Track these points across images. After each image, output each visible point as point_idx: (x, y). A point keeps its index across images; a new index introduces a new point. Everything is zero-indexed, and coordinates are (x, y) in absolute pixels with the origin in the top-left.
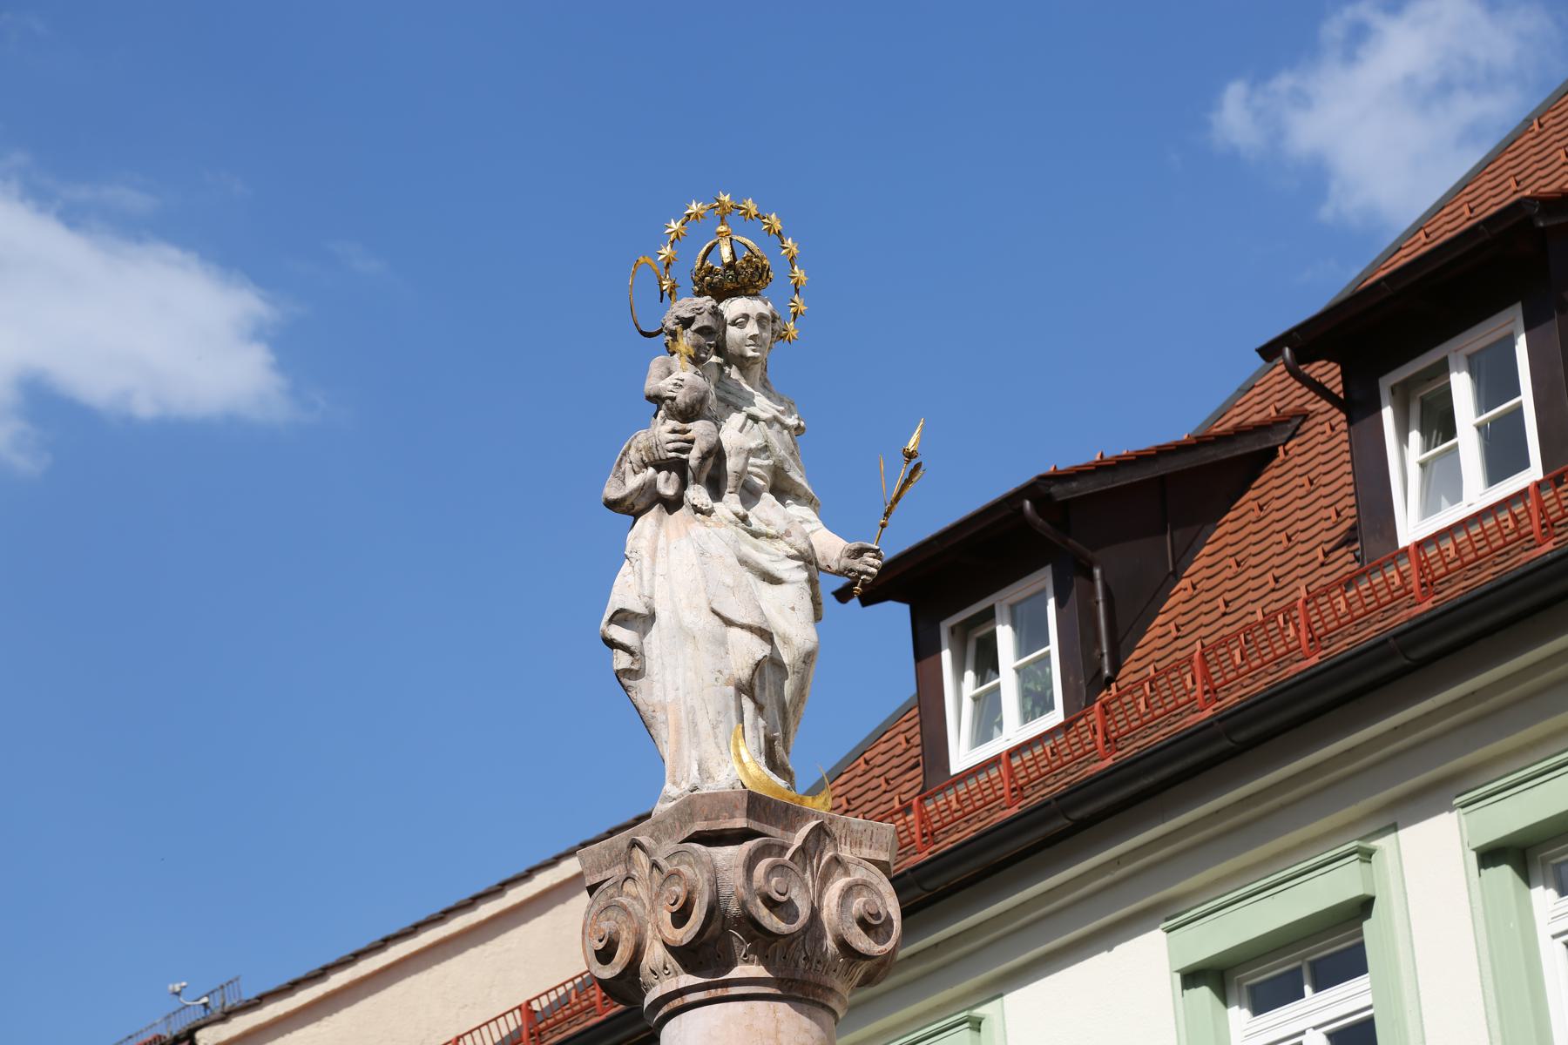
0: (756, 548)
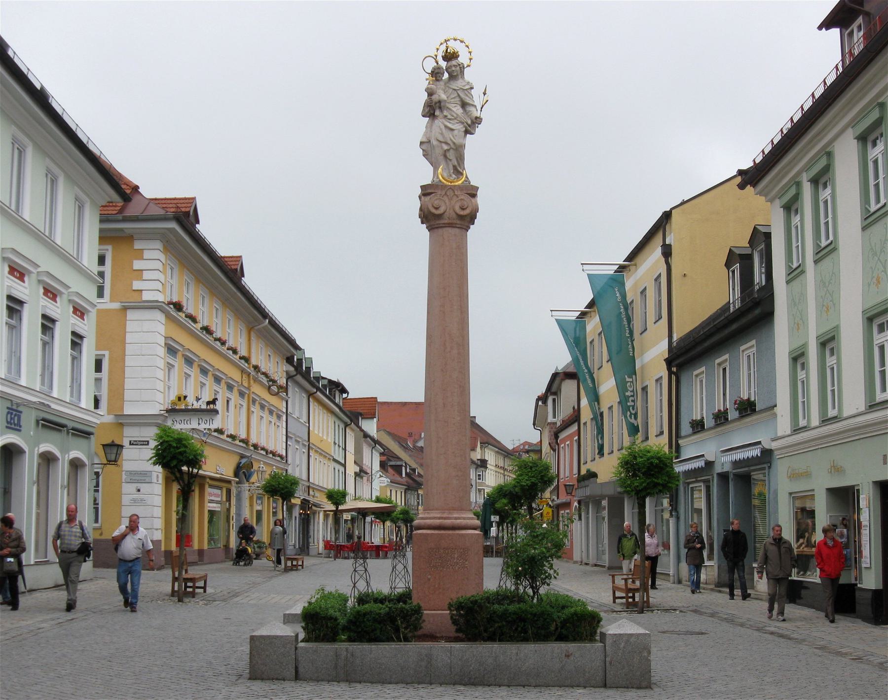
0: (450, 123)
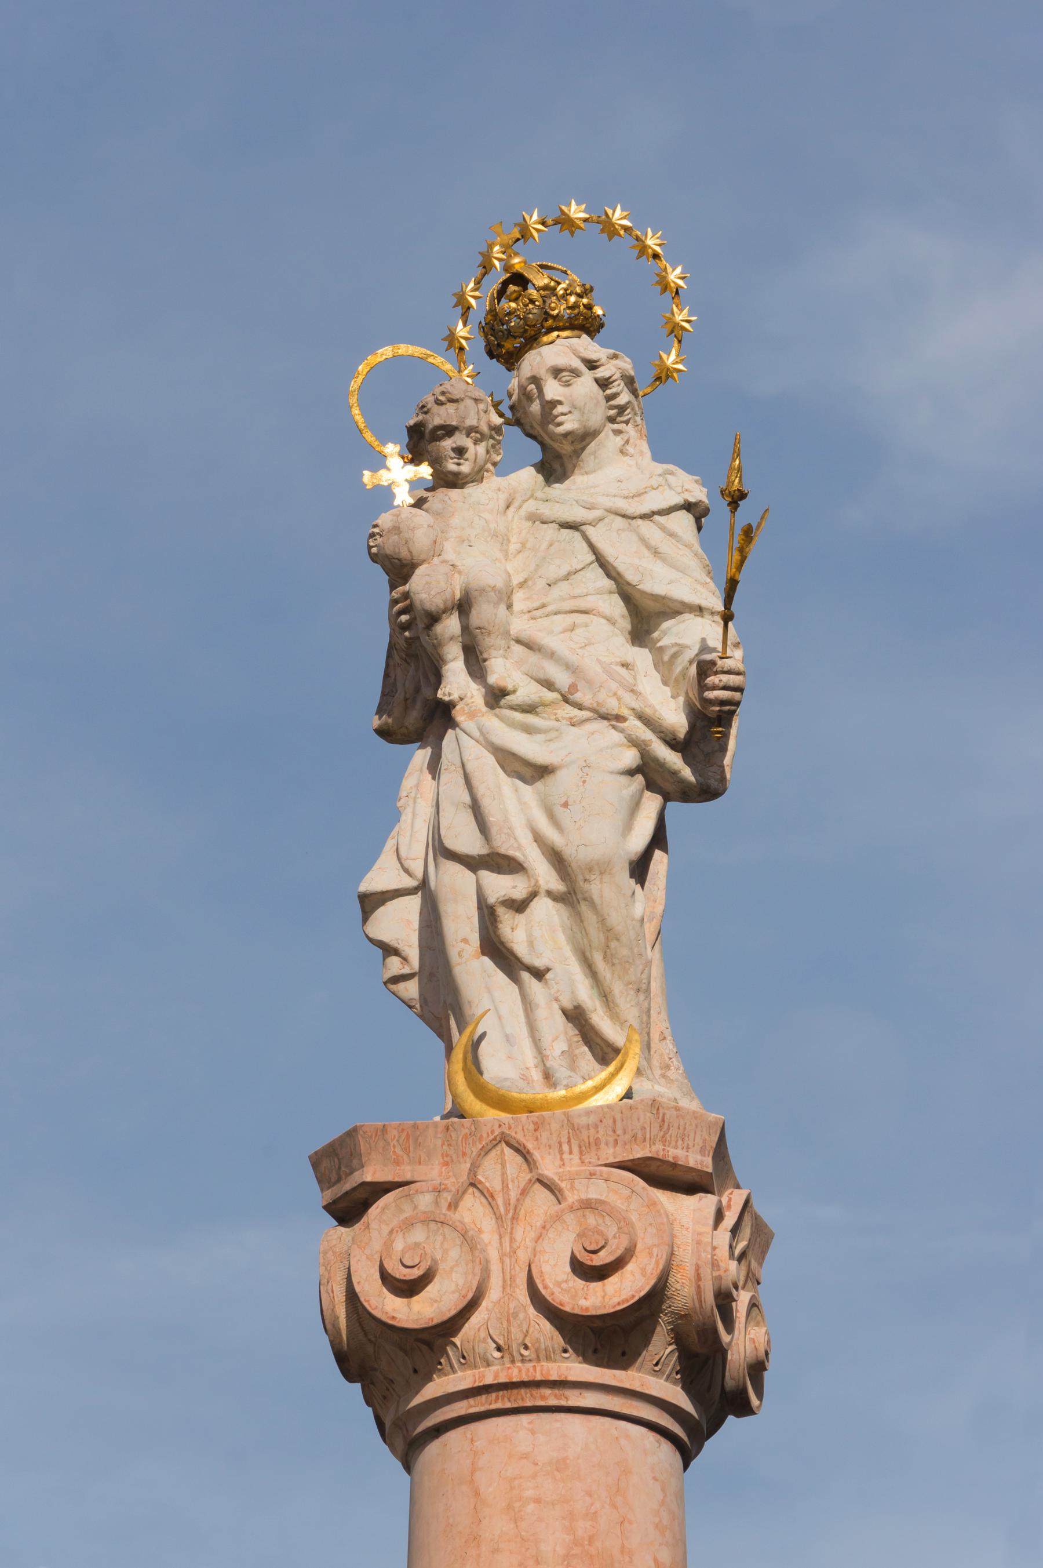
0: (529, 730)
